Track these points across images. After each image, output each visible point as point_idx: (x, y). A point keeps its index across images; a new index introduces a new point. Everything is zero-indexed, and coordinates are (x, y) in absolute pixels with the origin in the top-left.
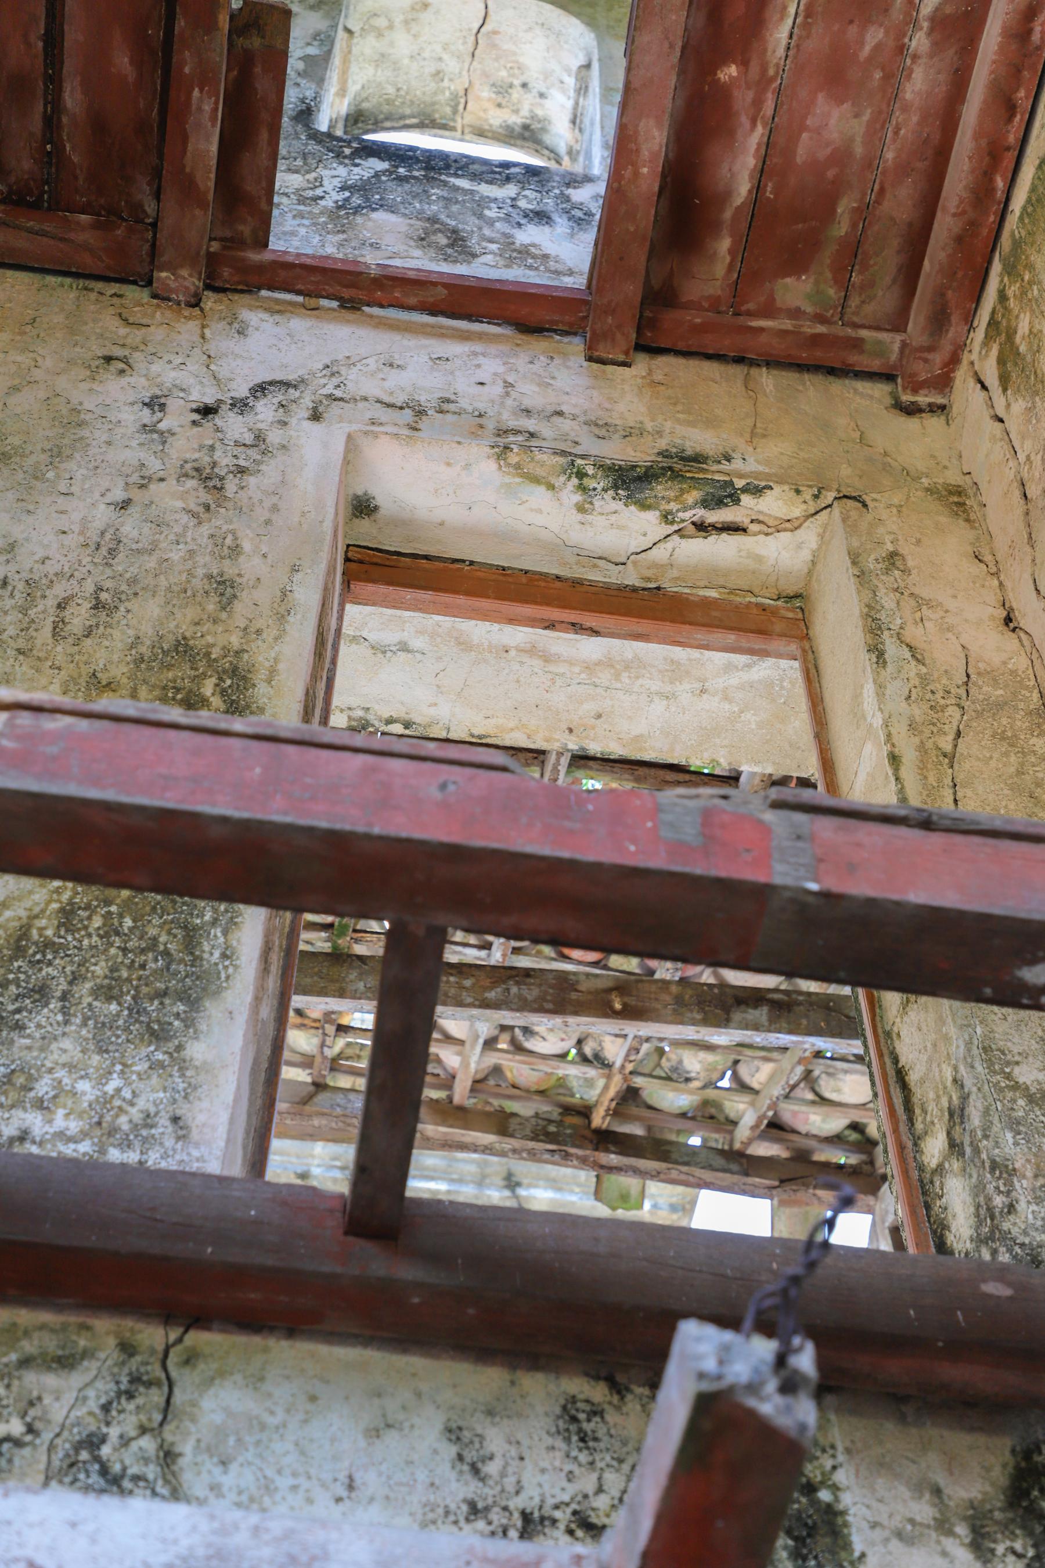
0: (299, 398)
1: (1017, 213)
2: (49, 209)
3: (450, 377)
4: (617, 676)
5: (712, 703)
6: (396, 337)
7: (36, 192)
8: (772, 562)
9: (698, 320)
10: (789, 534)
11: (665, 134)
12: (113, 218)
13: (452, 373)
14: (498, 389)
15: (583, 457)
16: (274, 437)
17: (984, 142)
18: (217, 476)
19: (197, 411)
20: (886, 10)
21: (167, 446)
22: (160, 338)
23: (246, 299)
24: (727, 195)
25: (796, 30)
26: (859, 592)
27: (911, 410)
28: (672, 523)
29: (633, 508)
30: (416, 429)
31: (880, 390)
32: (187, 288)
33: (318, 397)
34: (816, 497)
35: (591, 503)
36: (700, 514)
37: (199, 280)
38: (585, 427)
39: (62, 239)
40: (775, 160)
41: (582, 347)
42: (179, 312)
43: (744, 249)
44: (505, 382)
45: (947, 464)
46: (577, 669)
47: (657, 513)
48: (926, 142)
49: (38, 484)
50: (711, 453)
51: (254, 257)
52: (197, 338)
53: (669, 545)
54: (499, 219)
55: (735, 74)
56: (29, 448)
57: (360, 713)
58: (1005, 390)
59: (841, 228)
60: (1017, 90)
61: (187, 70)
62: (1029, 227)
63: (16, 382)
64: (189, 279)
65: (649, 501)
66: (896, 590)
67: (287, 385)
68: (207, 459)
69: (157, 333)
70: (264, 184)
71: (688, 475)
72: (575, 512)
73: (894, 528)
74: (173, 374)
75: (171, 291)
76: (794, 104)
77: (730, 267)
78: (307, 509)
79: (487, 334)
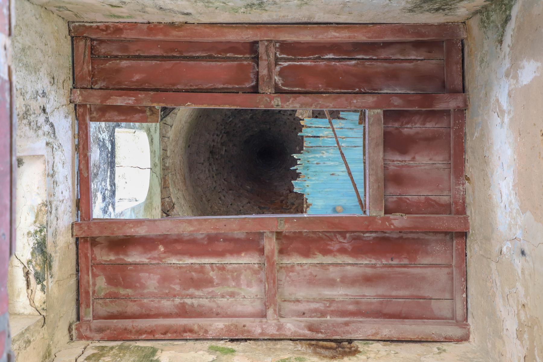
0: (52, 138)
1: (136, 345)
2: (91, 57)
3: (63, 183)
6: (71, 164)
7: (95, 53)
8: (18, 300)
9: (89, 255)
10: (29, 303)
11: (144, 234)
12: (92, 76)
13: (64, 183)
14: (61, 199)
15: (47, 231)
16: (40, 132)
17: (155, 328)
18: (27, 117)
19: (44, 107)
20: (184, 289)
21: (33, 99)
22: (61, 92)
23: (74, 116)
24: (127, 255)
25: (175, 265)
26: (17, 335)
27: (70, 330)
28: (28, 264)
29: (31, 250)
30: (48, 176)
31: (74, 317)
32: (75, 99)
33: (52, 143)
34: (43, 309)
35: (31, 236)
36: (32, 272)
37: (79, 103)
38: (55, 229)
39: (84, 62)
40: (139, 267)
41: (75, 221)
42: (68, 97)
43: (112, 264)
44: (63, 200)
45: (57, 347)
47: (31, 258)
48: (151, 310)
49: (17, 61)
50: (52, 271)
51: (88, 118)
52: (62, 103)
53: (20, 265)
54: (102, 186)
55: (161, 250)
56: (27, 57)
58: (86, 359)
59: (122, 292)
60: (170, 333)
61: (139, 95)
62: (135, 350)
63: (44, 51)
64: (78, 100)
65: (35, 255)
66: (20, 347)
67: (54, 133)
68: (31, 113)
69: (62, 92)
70: (109, 119)
71: (46, 266)
72: (27, 231)
73: (38, 339)
74: (52, 98)
75: (74, 94)
76: (156, 269)
77: (107, 261)
78: (22, 147)
79: (75, 191)
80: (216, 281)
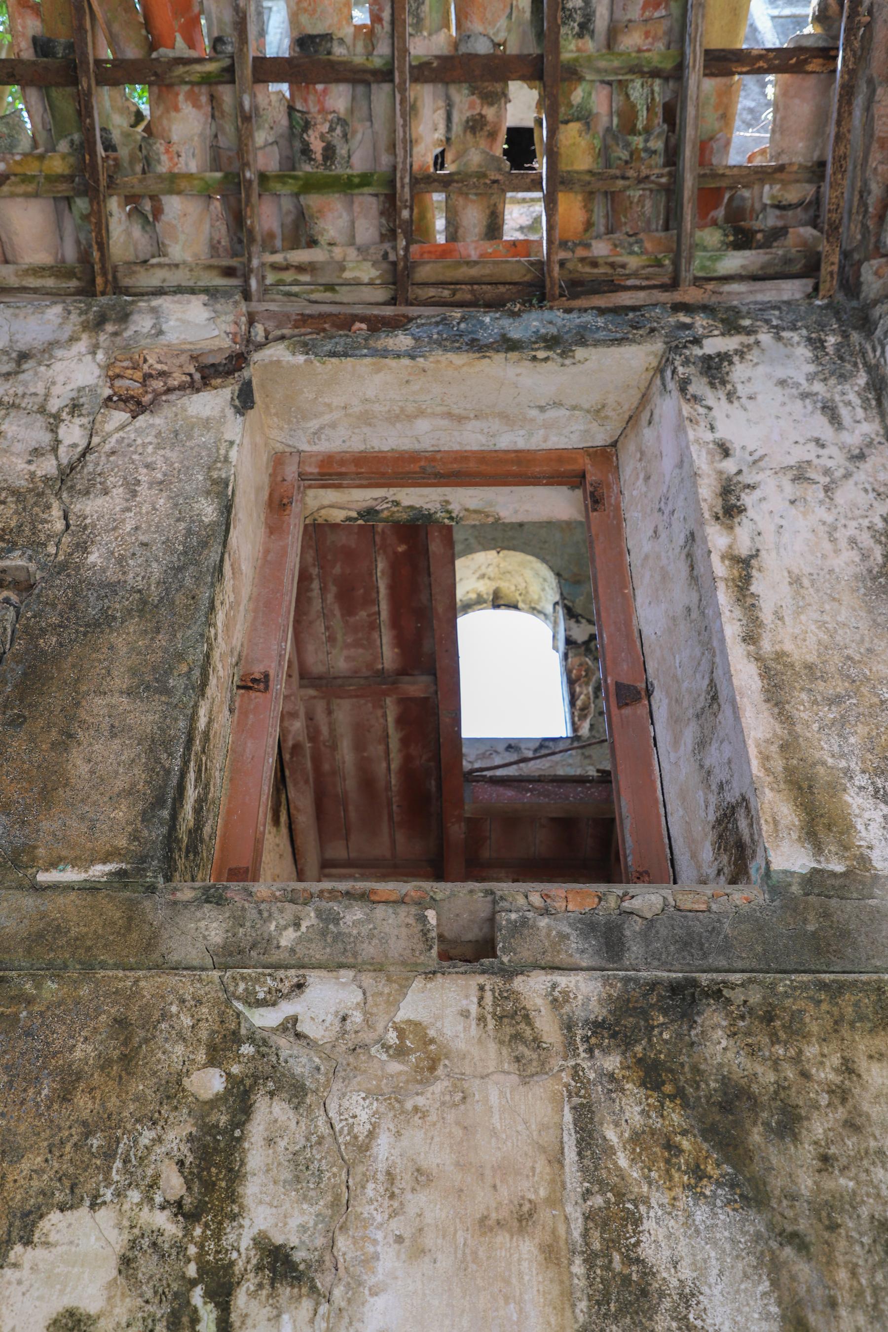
4: (402, 409)
5: (337, 401)
46: (429, 410)
57: (568, 362)
80: (352, 620)
